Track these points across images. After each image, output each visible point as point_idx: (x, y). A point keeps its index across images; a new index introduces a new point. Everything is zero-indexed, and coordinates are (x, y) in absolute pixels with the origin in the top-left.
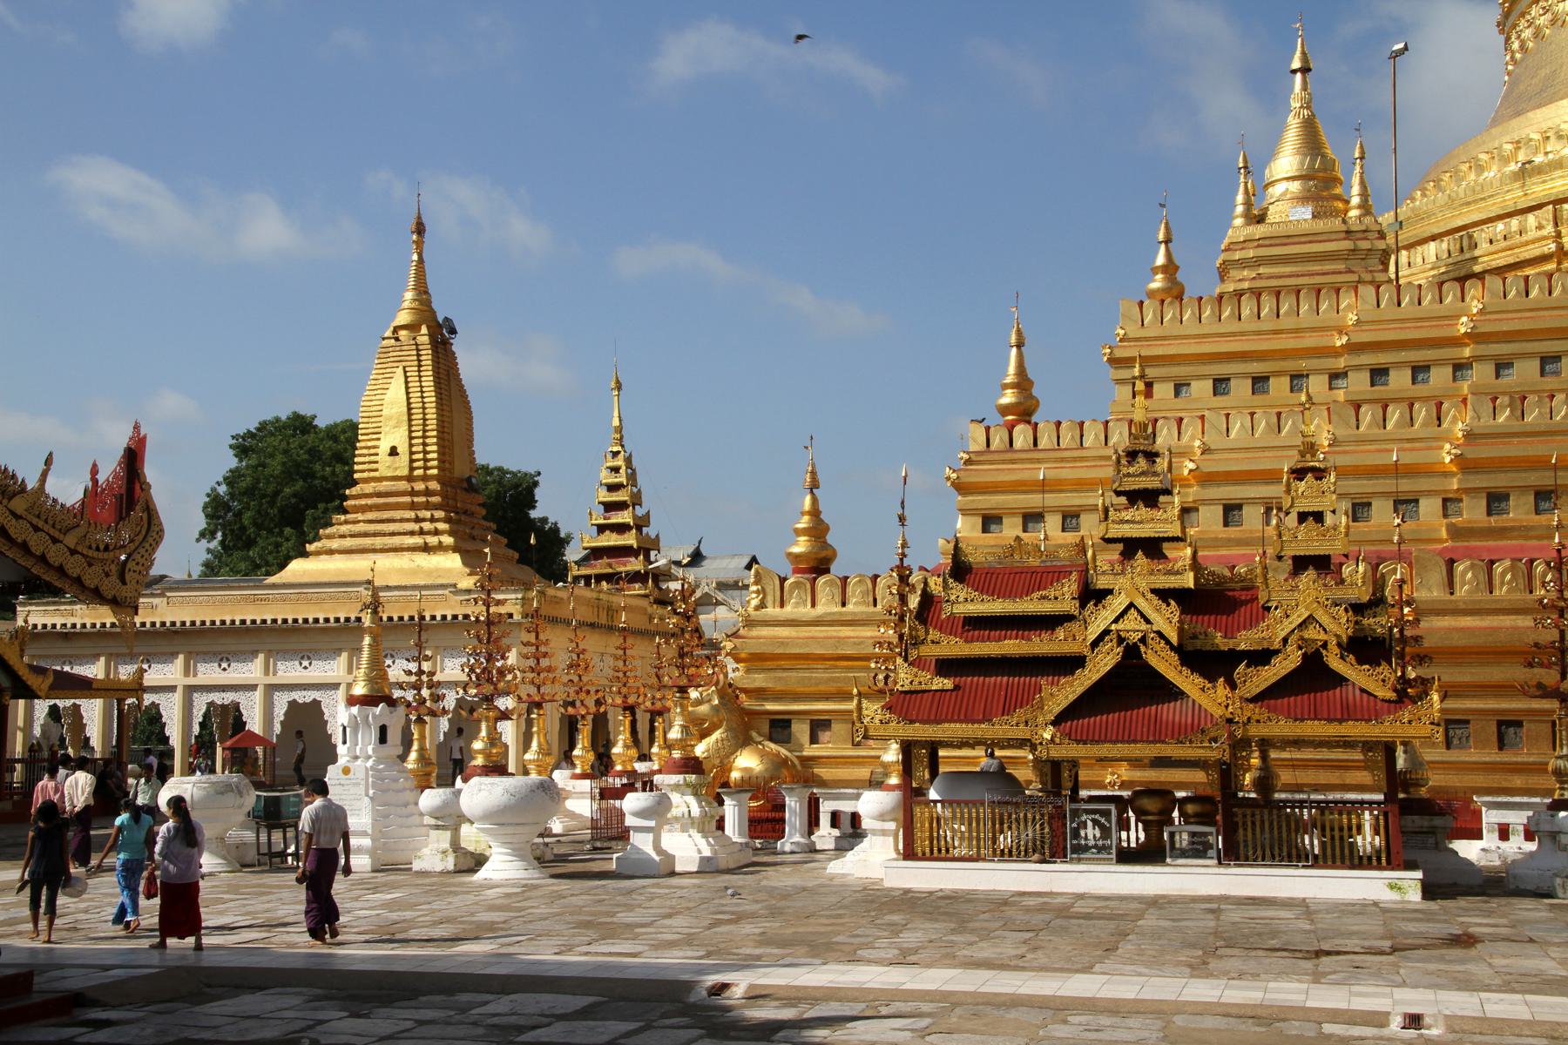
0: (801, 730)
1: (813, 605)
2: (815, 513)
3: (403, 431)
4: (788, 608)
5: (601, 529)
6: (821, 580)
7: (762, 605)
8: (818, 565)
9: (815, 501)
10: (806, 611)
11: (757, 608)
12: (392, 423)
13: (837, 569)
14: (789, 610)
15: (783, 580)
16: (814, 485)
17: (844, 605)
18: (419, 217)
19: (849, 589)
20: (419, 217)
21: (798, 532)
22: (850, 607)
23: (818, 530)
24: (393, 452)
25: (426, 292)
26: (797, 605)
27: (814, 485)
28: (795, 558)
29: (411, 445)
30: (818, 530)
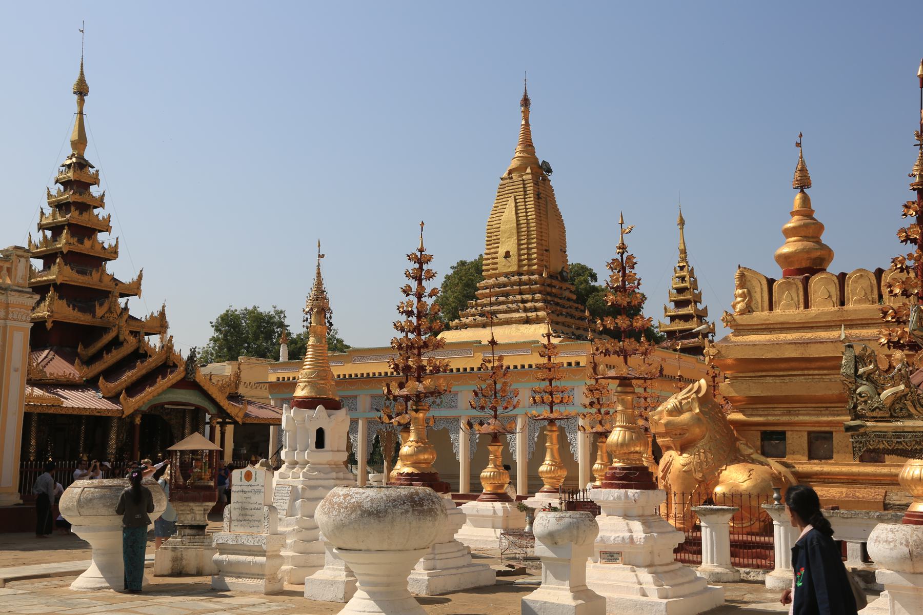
0: (797, 440)
1: (807, 306)
2: (806, 211)
3: (514, 239)
4: (778, 311)
5: (673, 318)
6: (815, 280)
7: (748, 309)
8: (808, 266)
9: (806, 200)
10: (795, 313)
11: (742, 313)
12: (506, 235)
13: (834, 268)
14: (781, 313)
15: (771, 282)
16: (803, 184)
17: (842, 303)
18: (526, 95)
19: (848, 290)
20: (526, 95)
21: (788, 233)
22: (850, 306)
23: (810, 229)
24: (507, 255)
25: (531, 146)
26: (788, 306)
27: (803, 184)
28: (784, 259)
29: (519, 250)
30: (810, 229)
